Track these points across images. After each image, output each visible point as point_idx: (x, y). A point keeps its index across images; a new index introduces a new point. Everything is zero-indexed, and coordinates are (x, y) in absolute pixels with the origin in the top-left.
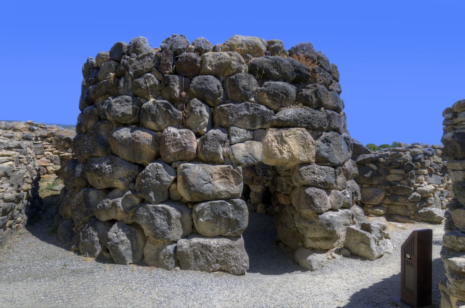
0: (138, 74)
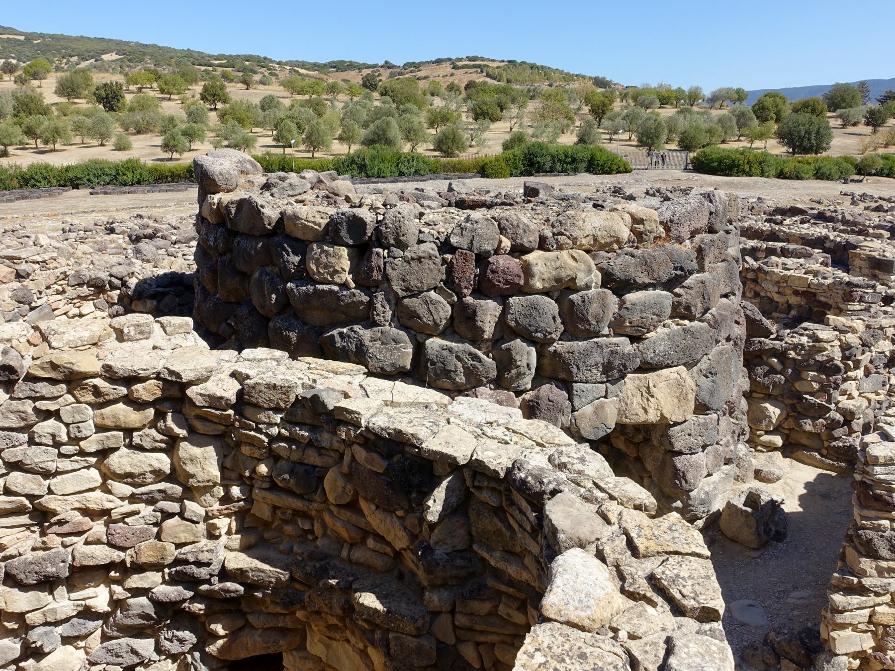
0: (413, 293)
